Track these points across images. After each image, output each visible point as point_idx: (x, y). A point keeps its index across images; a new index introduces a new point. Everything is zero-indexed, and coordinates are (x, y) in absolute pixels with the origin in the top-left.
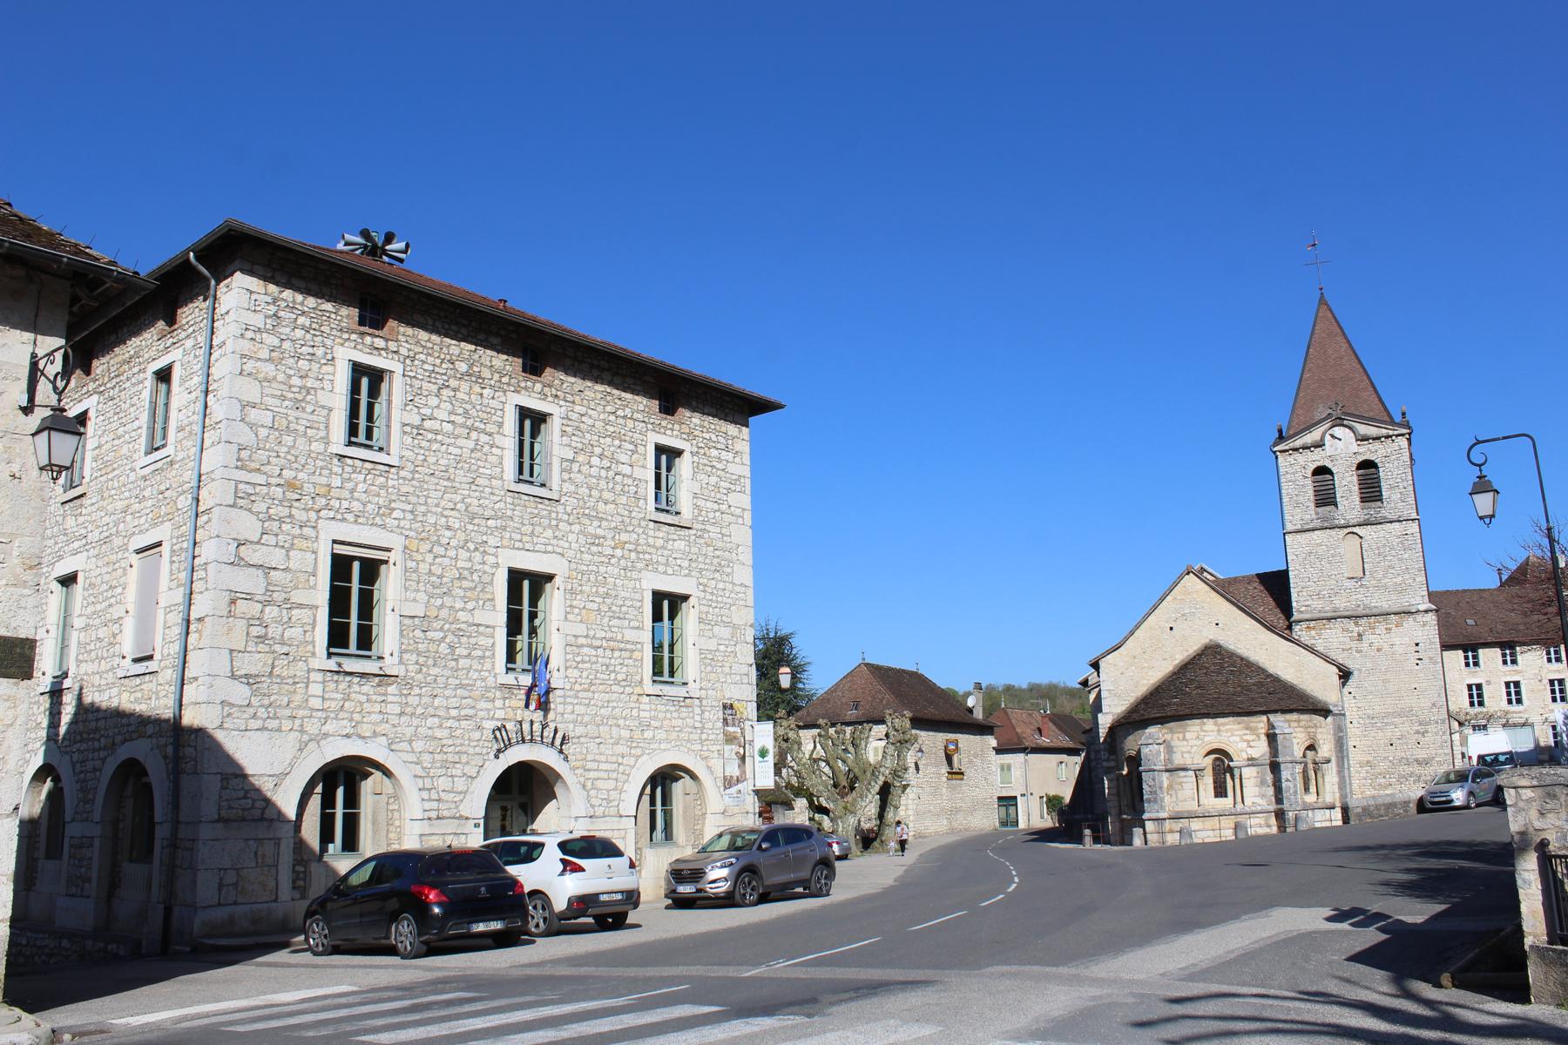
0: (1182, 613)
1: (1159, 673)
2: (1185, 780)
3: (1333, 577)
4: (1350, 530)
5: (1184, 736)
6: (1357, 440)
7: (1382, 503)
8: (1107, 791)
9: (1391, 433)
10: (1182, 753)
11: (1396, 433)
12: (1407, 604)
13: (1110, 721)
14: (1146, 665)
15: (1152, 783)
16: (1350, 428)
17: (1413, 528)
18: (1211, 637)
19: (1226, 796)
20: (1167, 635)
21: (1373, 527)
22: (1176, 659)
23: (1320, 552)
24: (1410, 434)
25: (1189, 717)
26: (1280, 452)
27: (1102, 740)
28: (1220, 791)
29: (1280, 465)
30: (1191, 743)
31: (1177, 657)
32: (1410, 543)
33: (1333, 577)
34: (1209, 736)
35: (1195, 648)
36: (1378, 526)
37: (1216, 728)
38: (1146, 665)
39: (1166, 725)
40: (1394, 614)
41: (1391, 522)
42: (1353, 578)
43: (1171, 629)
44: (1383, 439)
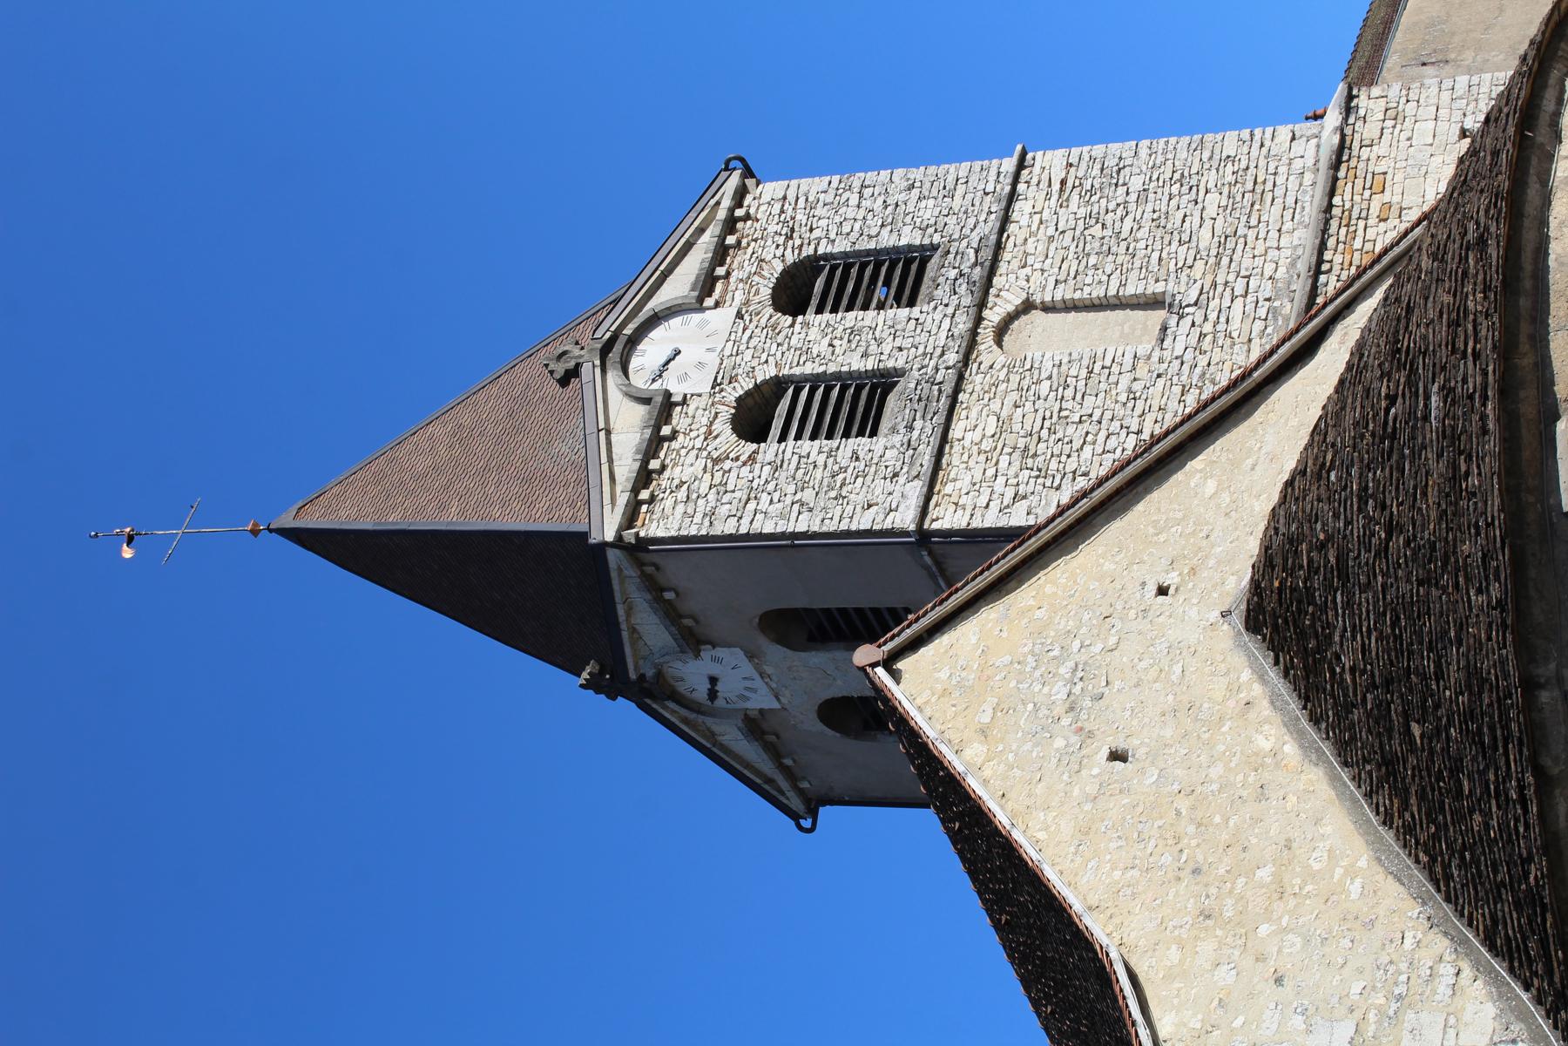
0: (1059, 709)
1: (1329, 830)
3: (1137, 386)
6: (699, 307)
9: (722, 214)
11: (726, 203)
14: (1264, 874)
16: (655, 320)
17: (1049, 162)
18: (1214, 615)
20: (1142, 771)
21: (1003, 268)
22: (1275, 754)
24: (748, 173)
25: (1529, 237)
26: (631, 517)
29: (673, 533)
31: (1265, 744)
32: (1096, 171)
35: (1246, 675)
36: (1006, 256)
38: (1264, 874)
41: (1005, 220)
42: (1164, 329)
43: (1117, 756)
44: (731, 240)
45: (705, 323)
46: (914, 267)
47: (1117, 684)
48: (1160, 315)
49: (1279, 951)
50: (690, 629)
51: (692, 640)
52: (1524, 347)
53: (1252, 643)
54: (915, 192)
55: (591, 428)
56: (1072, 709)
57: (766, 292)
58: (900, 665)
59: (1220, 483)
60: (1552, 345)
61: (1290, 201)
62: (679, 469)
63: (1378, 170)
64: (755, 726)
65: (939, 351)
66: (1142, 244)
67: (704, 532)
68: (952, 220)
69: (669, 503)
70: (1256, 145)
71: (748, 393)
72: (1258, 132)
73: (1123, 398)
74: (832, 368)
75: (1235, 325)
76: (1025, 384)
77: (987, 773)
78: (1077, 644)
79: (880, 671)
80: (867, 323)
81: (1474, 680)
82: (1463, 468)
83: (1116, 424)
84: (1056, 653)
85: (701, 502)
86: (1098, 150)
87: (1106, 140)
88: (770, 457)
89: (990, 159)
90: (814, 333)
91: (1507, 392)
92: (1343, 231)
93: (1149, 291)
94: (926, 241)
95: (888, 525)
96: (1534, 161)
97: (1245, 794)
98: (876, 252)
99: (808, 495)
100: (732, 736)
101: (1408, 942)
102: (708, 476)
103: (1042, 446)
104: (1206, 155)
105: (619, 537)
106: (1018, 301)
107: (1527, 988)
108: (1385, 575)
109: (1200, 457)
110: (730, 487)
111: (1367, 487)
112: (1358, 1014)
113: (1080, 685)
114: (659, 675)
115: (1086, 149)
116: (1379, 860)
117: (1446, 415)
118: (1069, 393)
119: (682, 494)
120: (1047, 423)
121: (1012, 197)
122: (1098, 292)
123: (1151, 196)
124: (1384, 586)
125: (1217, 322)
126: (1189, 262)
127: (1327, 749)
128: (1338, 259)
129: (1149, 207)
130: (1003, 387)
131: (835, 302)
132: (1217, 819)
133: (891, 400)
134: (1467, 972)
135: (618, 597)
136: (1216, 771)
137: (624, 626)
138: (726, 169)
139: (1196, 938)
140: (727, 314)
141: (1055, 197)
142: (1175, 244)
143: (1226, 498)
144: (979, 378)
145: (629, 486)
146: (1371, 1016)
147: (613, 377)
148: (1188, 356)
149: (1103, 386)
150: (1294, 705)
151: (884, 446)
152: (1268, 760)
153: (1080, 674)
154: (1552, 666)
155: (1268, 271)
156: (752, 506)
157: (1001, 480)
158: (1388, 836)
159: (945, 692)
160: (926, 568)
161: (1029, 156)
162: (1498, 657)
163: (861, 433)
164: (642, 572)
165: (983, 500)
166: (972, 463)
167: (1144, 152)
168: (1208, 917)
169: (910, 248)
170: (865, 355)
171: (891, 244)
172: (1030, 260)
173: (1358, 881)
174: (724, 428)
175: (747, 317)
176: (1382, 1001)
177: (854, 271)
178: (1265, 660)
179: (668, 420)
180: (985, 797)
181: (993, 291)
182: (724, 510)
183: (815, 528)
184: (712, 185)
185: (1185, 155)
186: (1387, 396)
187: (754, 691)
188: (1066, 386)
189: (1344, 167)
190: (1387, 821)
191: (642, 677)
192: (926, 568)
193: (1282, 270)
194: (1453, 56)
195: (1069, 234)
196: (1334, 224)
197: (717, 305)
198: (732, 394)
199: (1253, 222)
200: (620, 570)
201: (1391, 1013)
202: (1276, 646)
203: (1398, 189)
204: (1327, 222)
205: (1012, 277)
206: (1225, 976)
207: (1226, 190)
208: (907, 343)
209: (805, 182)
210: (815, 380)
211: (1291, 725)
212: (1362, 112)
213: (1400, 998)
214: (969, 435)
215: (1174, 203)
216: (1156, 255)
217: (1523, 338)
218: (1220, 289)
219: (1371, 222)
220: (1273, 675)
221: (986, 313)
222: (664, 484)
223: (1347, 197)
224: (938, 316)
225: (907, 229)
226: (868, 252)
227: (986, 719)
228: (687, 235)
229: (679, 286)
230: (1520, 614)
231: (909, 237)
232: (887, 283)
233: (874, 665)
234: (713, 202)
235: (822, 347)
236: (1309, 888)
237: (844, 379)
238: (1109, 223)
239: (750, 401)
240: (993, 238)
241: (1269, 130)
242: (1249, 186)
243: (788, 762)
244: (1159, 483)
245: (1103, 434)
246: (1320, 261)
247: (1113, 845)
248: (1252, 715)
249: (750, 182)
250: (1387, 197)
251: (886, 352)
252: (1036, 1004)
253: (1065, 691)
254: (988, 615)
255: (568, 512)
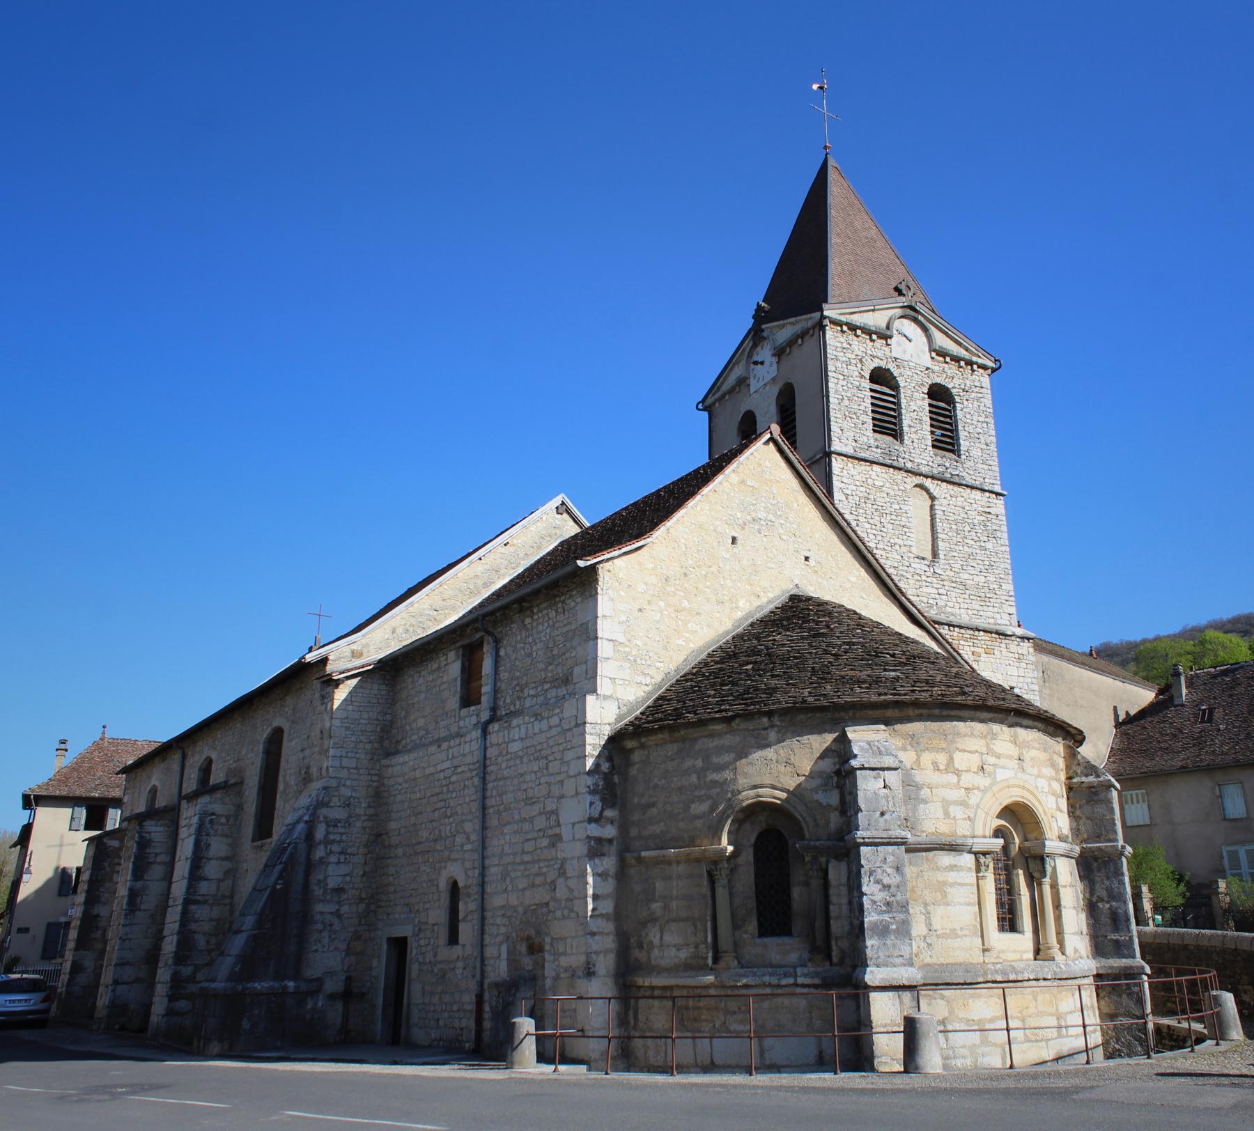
0: (753, 515)
2: (952, 877)
3: (897, 547)
4: (920, 480)
5: (951, 759)
6: (930, 351)
7: (959, 456)
8: (590, 907)
9: (975, 359)
10: (946, 804)
11: (979, 361)
12: (992, 621)
13: (612, 719)
14: (685, 604)
15: (892, 879)
16: (925, 330)
17: (999, 506)
19: (1022, 932)
21: (951, 487)
23: (880, 502)
24: (994, 370)
25: (966, 713)
27: (589, 763)
28: (1009, 922)
30: (967, 780)
32: (994, 528)
33: (897, 547)
34: (1002, 767)
35: (771, 595)
36: (956, 488)
37: (1015, 752)
38: (685, 604)
39: (898, 727)
40: (985, 631)
41: (972, 487)
42: (923, 559)
43: (734, 540)
44: (962, 363)
45: (922, 351)
46: (950, 447)
47: (765, 540)
48: (930, 557)
49: (653, 610)
50: (785, 351)
51: (780, 353)
52: (917, 712)
53: (785, 598)
54: (985, 447)
55: (875, 302)
56: (754, 520)
57: (938, 381)
58: (771, 444)
59: (855, 583)
60: (918, 723)
61: (981, 613)
62: (857, 343)
63: (995, 651)
64: (743, 382)
65: (912, 459)
66: (961, 548)
67: (828, 356)
68: (972, 463)
69: (842, 339)
70: (1007, 598)
71: (892, 374)
72: (1013, 599)
73: (892, 541)
74: (903, 411)
75: (925, 589)
76: (898, 498)
77: (725, 484)
78: (783, 522)
79: (768, 436)
80: (924, 427)
81: (771, 691)
82: (864, 686)
83: (880, 538)
84: (778, 513)
85: (842, 354)
86: (1004, 528)
87: (1009, 532)
88: (863, 385)
89: (1001, 480)
90: (919, 403)
91: (897, 704)
92: (968, 636)
93: (940, 552)
94: (962, 452)
95: (833, 438)
96: (1001, 716)
97: (719, 595)
98: (957, 430)
99: (846, 402)
100: (738, 372)
101: (658, 665)
102: (854, 357)
103: (870, 506)
104: (1002, 576)
105: (826, 317)
106: (935, 494)
107: (641, 713)
108: (816, 653)
109: (866, 575)
110: (849, 367)
111: (854, 645)
112: (627, 643)
113: (764, 523)
114: (764, 338)
115: (1005, 523)
116: (693, 652)
117: (886, 679)
118: (894, 517)
119: (845, 345)
120: (880, 508)
121: (983, 490)
122: (939, 529)
123: (983, 552)
124: (811, 653)
125: (926, 582)
126: (953, 569)
127: (740, 630)
128: (955, 634)
129: (978, 551)
130: (896, 488)
131: (934, 413)
132: (708, 583)
133: (890, 438)
134: (648, 689)
135: (798, 318)
136: (729, 583)
137: (785, 321)
138: (995, 360)
139: (657, 575)
140: (929, 363)
141: (983, 510)
142: (962, 563)
143: (848, 585)
144: (900, 477)
145: (849, 321)
146: (627, 649)
147: (899, 312)
148: (911, 569)
149: (897, 532)
150: (758, 616)
151: (868, 436)
152: (734, 605)
153: (769, 523)
154: (778, 723)
155: (950, 604)
156: (841, 377)
157: (854, 488)
158: (703, 656)
159: (760, 465)
160: (814, 456)
161: (1001, 498)
162: (782, 700)
163: (874, 425)
164: (809, 329)
165: (845, 480)
166: (861, 475)
167: (1003, 548)
168: (666, 580)
169: (959, 445)
170: (910, 426)
171: (961, 436)
172: (953, 499)
173: (684, 643)
174: (877, 363)
175: (927, 372)
176: (634, 654)
177: (948, 420)
178: (778, 603)
179: (879, 337)
180: (715, 483)
181: (940, 482)
182: (839, 364)
183: (831, 406)
184: (988, 354)
185: (1002, 566)
186: (894, 654)
187: (758, 381)
188: (897, 516)
189: (997, 636)
190: (709, 655)
191: (763, 331)
192: (814, 456)
193: (950, 610)
194: (1047, 685)
195: (966, 516)
196: (971, 632)
197: (932, 358)
198: (892, 367)
199: (971, 597)
200: (811, 318)
201: (629, 657)
202: (783, 608)
203: (987, 660)
204: (972, 629)
205: (946, 491)
206: (642, 587)
207: (986, 585)
208: (915, 445)
209: (989, 397)
210: (898, 404)
211: (750, 614)
212: (1022, 644)
213: (635, 661)
214: (874, 473)
215: (980, 562)
216: (957, 555)
217: (921, 711)
218: (941, 583)
219: (972, 649)
220: (771, 607)
221: (929, 480)
222: (850, 337)
223: (983, 638)
224: (928, 458)
225: (968, 443)
226: (957, 426)
227: (749, 483)
228: (965, 343)
229: (941, 340)
230: (801, 710)
231: (964, 444)
232: (943, 435)
233: (771, 433)
234: (980, 354)
235: (913, 407)
236: (680, 622)
237: (899, 417)
238: (971, 534)
239: (888, 375)
240: (964, 482)
241: (1014, 604)
242: (988, 595)
243: (727, 397)
244: (854, 557)
245: (875, 532)
246: (954, 626)
247: (695, 539)
248: (753, 598)
249: (989, 371)
250: (983, 655)
251: (911, 436)
252: (626, 509)
253: (762, 517)
254: (794, 483)
255: (836, 293)
